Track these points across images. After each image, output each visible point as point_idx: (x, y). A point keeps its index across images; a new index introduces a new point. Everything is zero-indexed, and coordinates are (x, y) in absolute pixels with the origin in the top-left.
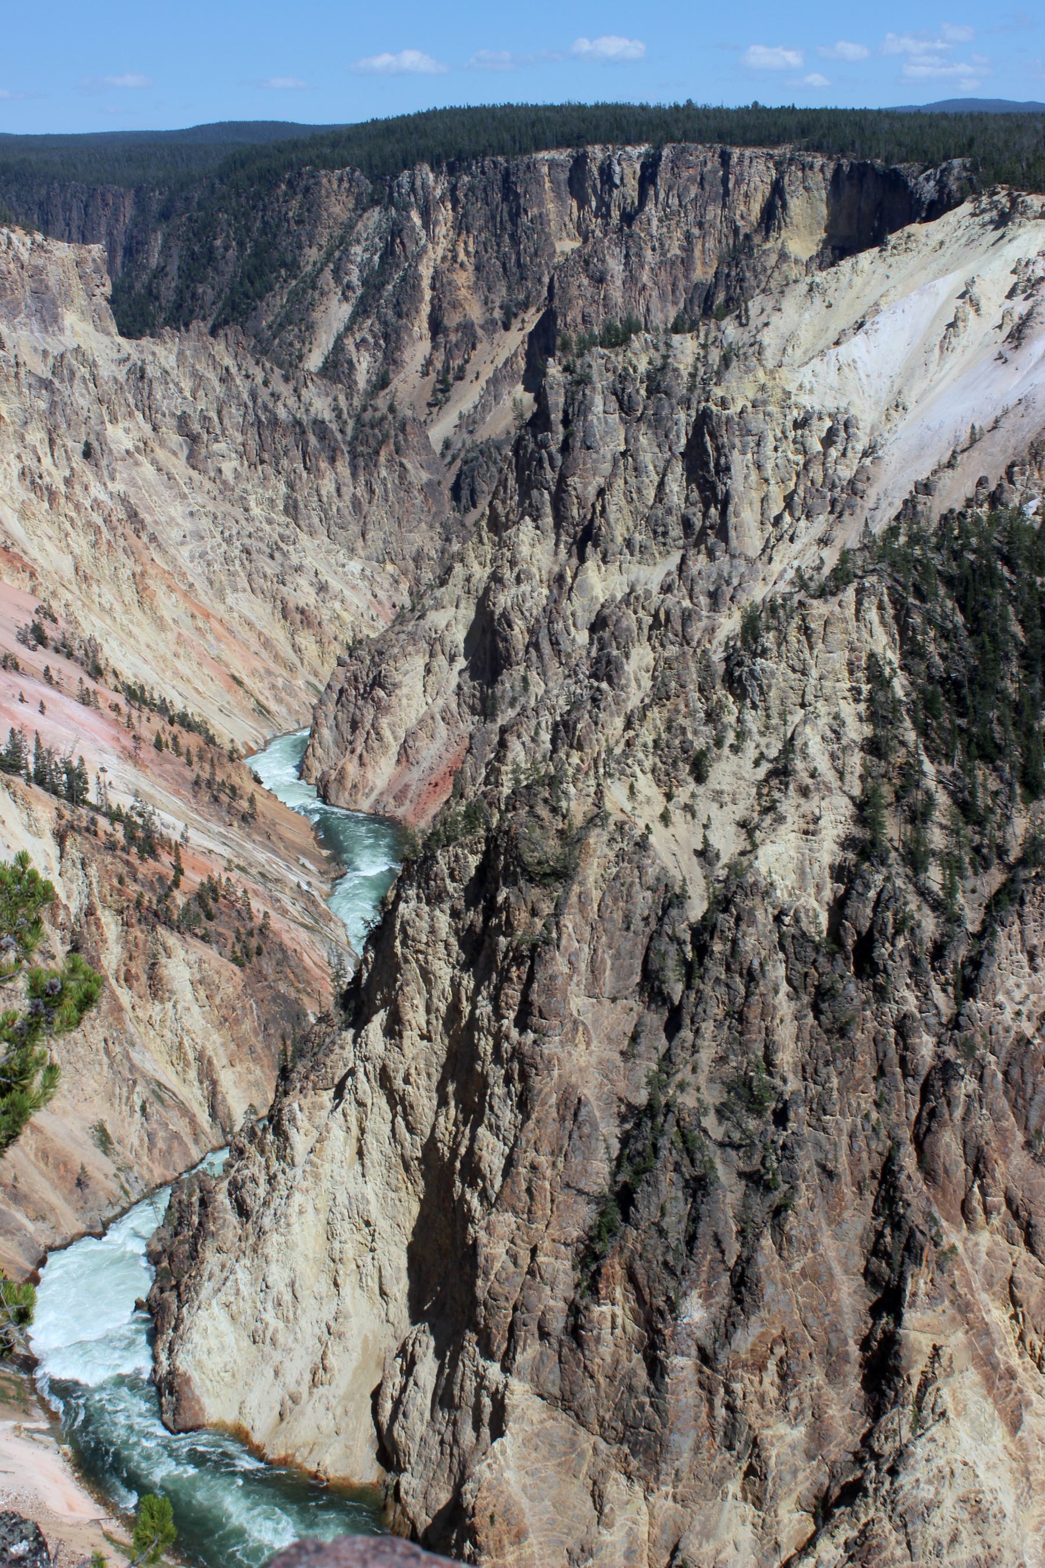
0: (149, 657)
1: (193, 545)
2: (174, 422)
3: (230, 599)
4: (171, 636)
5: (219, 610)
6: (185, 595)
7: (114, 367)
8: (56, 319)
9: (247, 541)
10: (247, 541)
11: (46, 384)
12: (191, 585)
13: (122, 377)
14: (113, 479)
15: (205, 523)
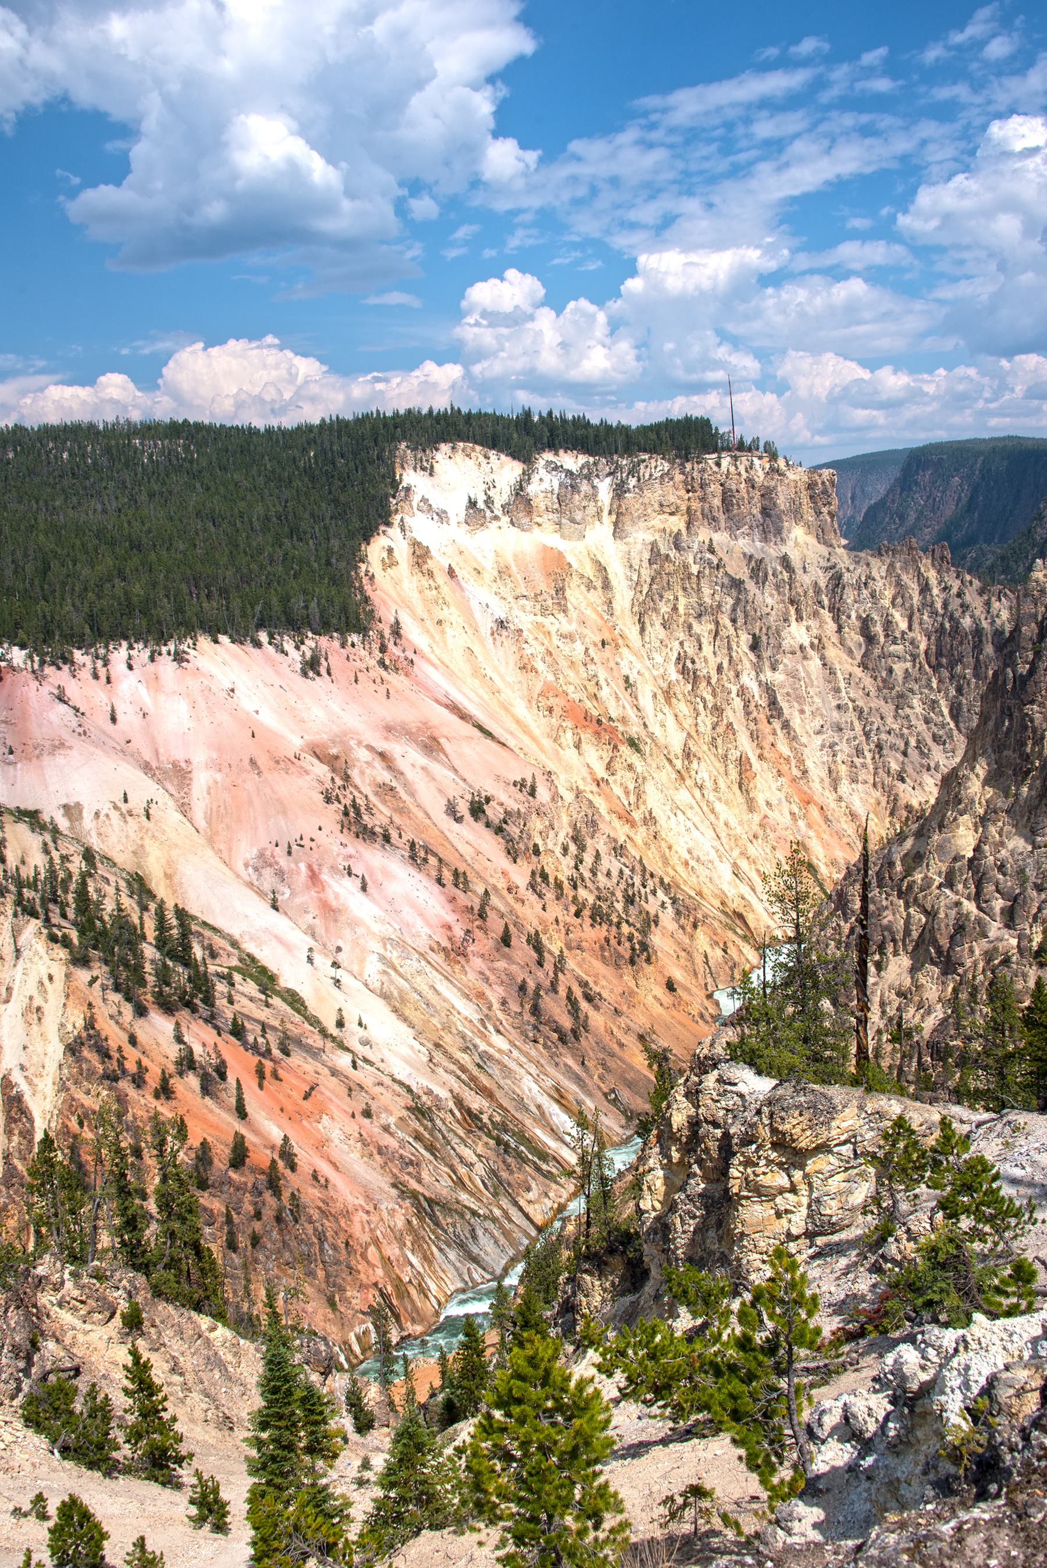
0: (723, 835)
1: (829, 735)
2: (858, 624)
3: (844, 787)
4: (757, 818)
5: (828, 798)
6: (794, 780)
7: (820, 573)
8: (779, 531)
9: (884, 736)
10: (884, 736)
11: (737, 584)
12: (805, 772)
13: (822, 584)
14: (774, 669)
15: (851, 716)
